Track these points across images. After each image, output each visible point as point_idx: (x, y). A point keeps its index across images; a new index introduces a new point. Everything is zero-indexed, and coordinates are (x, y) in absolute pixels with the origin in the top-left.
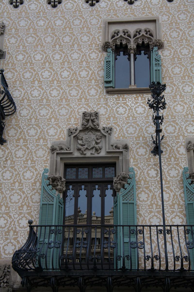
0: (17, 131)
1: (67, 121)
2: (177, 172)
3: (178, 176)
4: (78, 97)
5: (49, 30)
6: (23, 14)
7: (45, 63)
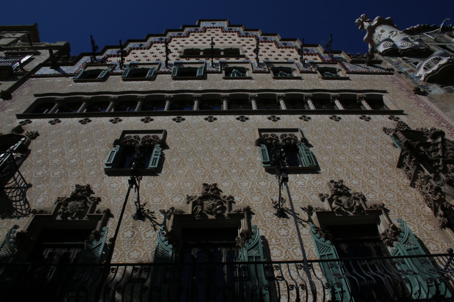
4: (77, 176)
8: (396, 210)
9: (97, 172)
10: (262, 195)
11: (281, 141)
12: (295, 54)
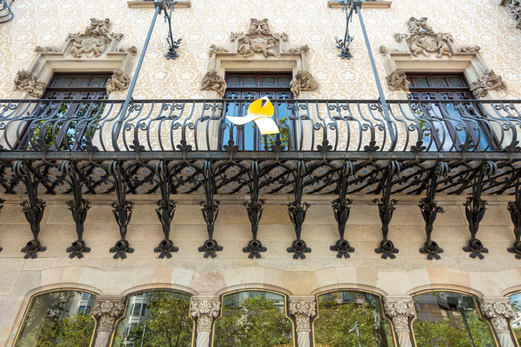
4: (93, 10)
8: (495, 55)
9: (118, 6)
10: (324, 34)
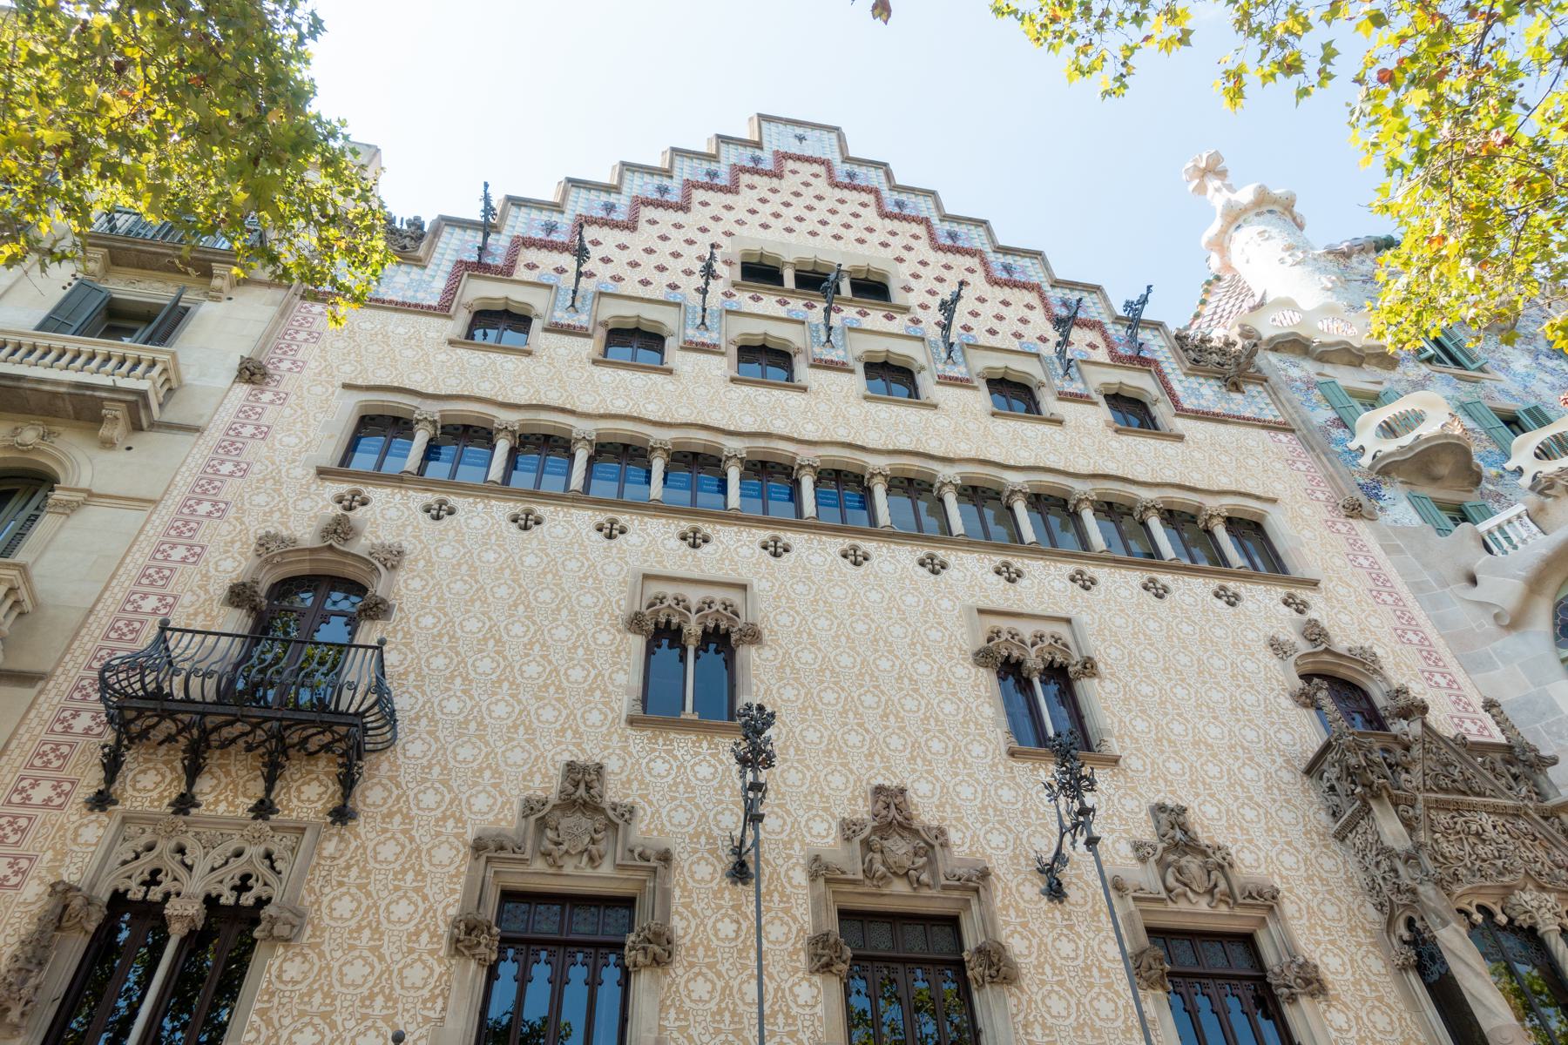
0: (391, 792)
1: (524, 779)
2: (785, 929)
3: (788, 939)
5: (507, 572)
6: (452, 533)
7: (485, 639)
11: (1033, 652)
12: (1040, 324)
